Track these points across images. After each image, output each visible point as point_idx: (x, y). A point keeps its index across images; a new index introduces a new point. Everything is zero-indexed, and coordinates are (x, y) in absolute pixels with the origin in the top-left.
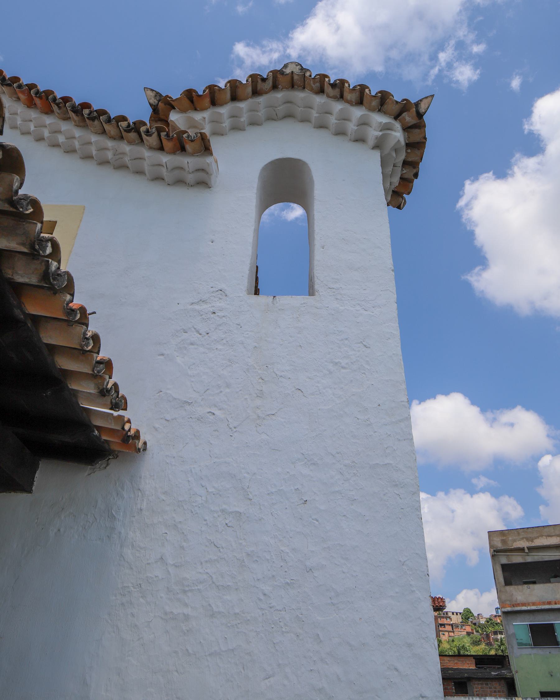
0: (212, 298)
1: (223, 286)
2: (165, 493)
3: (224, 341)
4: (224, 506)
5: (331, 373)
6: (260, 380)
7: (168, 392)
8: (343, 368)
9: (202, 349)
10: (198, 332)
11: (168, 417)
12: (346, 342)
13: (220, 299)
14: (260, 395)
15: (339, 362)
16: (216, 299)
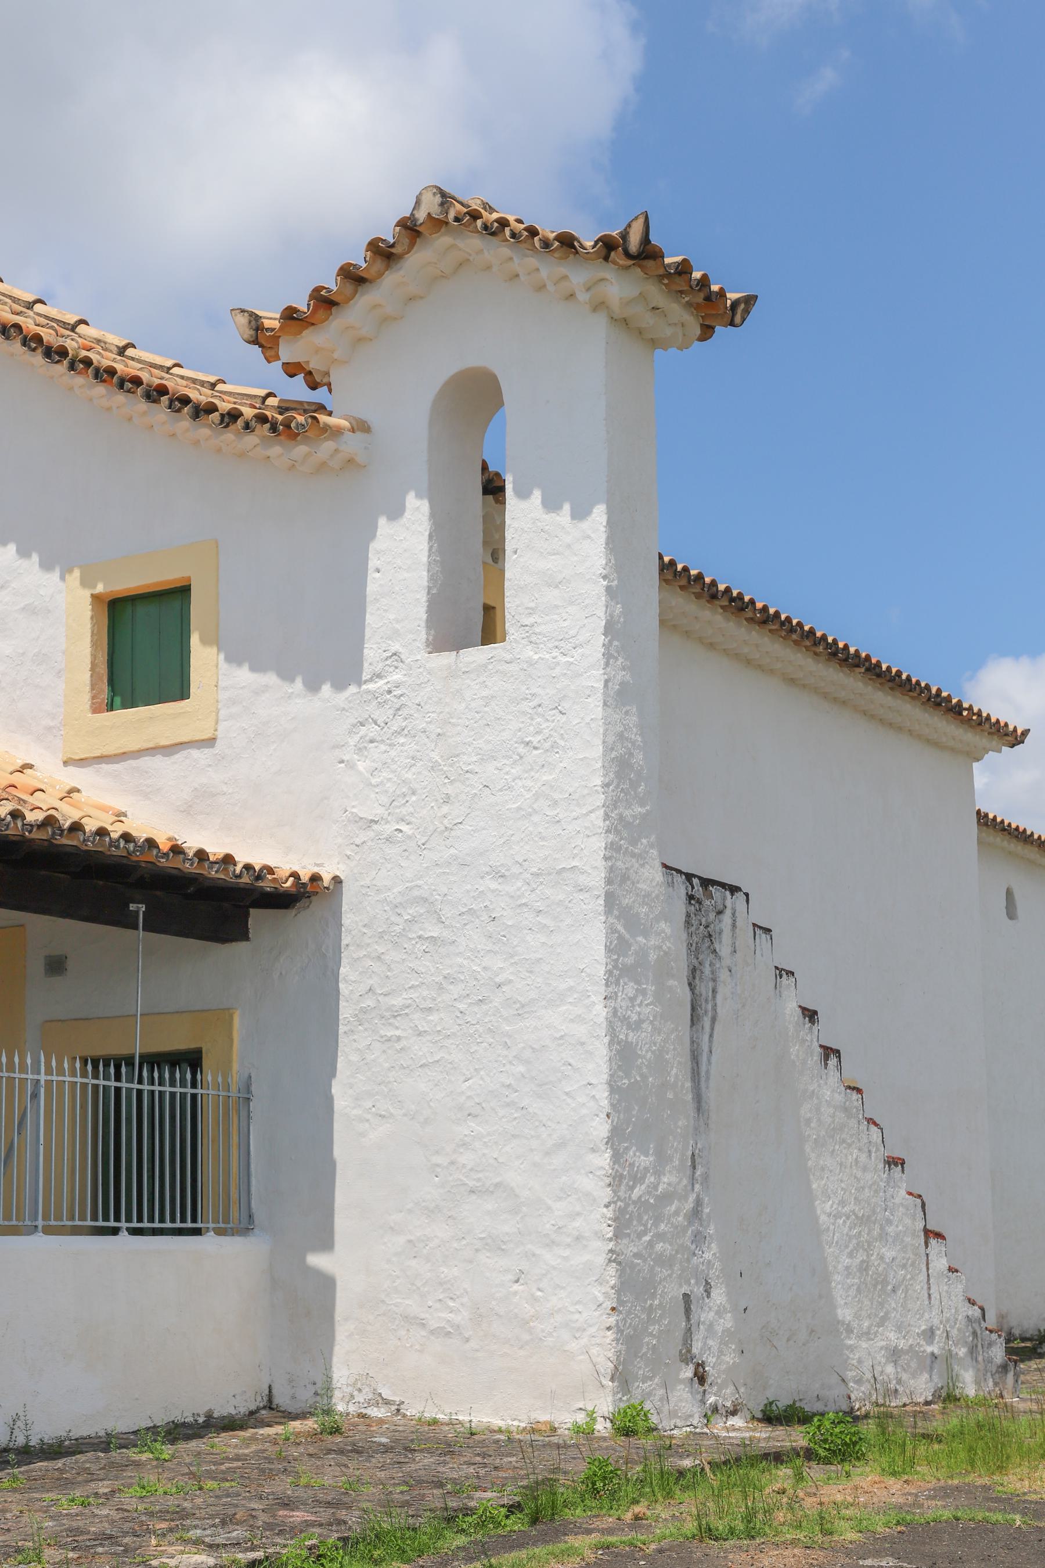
0: (387, 668)
1: (396, 647)
2: (365, 926)
3: (406, 732)
4: (421, 932)
5: (521, 757)
6: (446, 781)
7: (354, 810)
8: (535, 748)
9: (383, 747)
10: (376, 724)
11: (358, 841)
12: (540, 709)
13: (396, 668)
14: (447, 800)
15: (530, 741)
16: (391, 669)
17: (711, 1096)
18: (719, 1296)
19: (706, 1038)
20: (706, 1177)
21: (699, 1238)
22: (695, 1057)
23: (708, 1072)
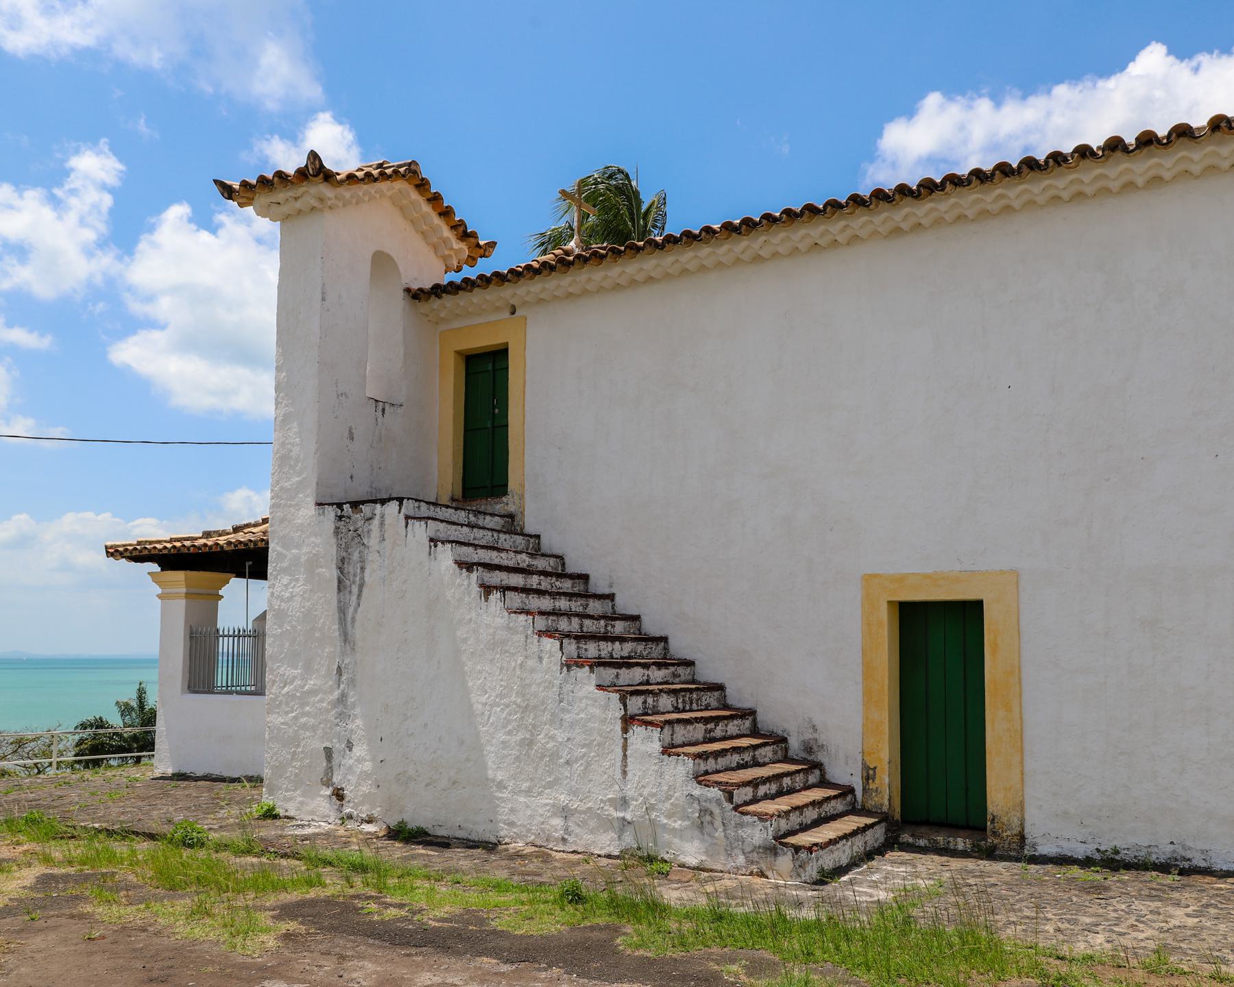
17: (357, 633)
18: (359, 750)
19: (354, 598)
20: (352, 682)
21: (342, 716)
22: (342, 610)
23: (353, 619)
